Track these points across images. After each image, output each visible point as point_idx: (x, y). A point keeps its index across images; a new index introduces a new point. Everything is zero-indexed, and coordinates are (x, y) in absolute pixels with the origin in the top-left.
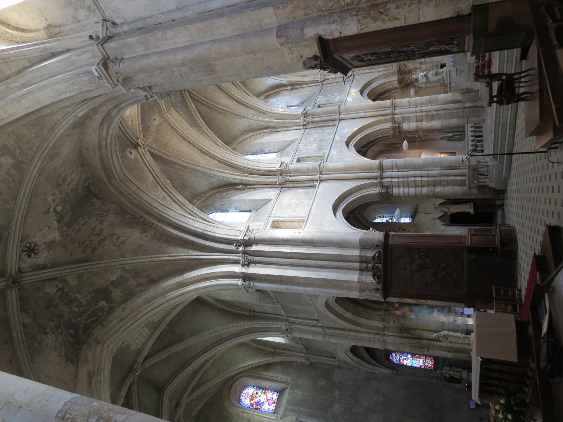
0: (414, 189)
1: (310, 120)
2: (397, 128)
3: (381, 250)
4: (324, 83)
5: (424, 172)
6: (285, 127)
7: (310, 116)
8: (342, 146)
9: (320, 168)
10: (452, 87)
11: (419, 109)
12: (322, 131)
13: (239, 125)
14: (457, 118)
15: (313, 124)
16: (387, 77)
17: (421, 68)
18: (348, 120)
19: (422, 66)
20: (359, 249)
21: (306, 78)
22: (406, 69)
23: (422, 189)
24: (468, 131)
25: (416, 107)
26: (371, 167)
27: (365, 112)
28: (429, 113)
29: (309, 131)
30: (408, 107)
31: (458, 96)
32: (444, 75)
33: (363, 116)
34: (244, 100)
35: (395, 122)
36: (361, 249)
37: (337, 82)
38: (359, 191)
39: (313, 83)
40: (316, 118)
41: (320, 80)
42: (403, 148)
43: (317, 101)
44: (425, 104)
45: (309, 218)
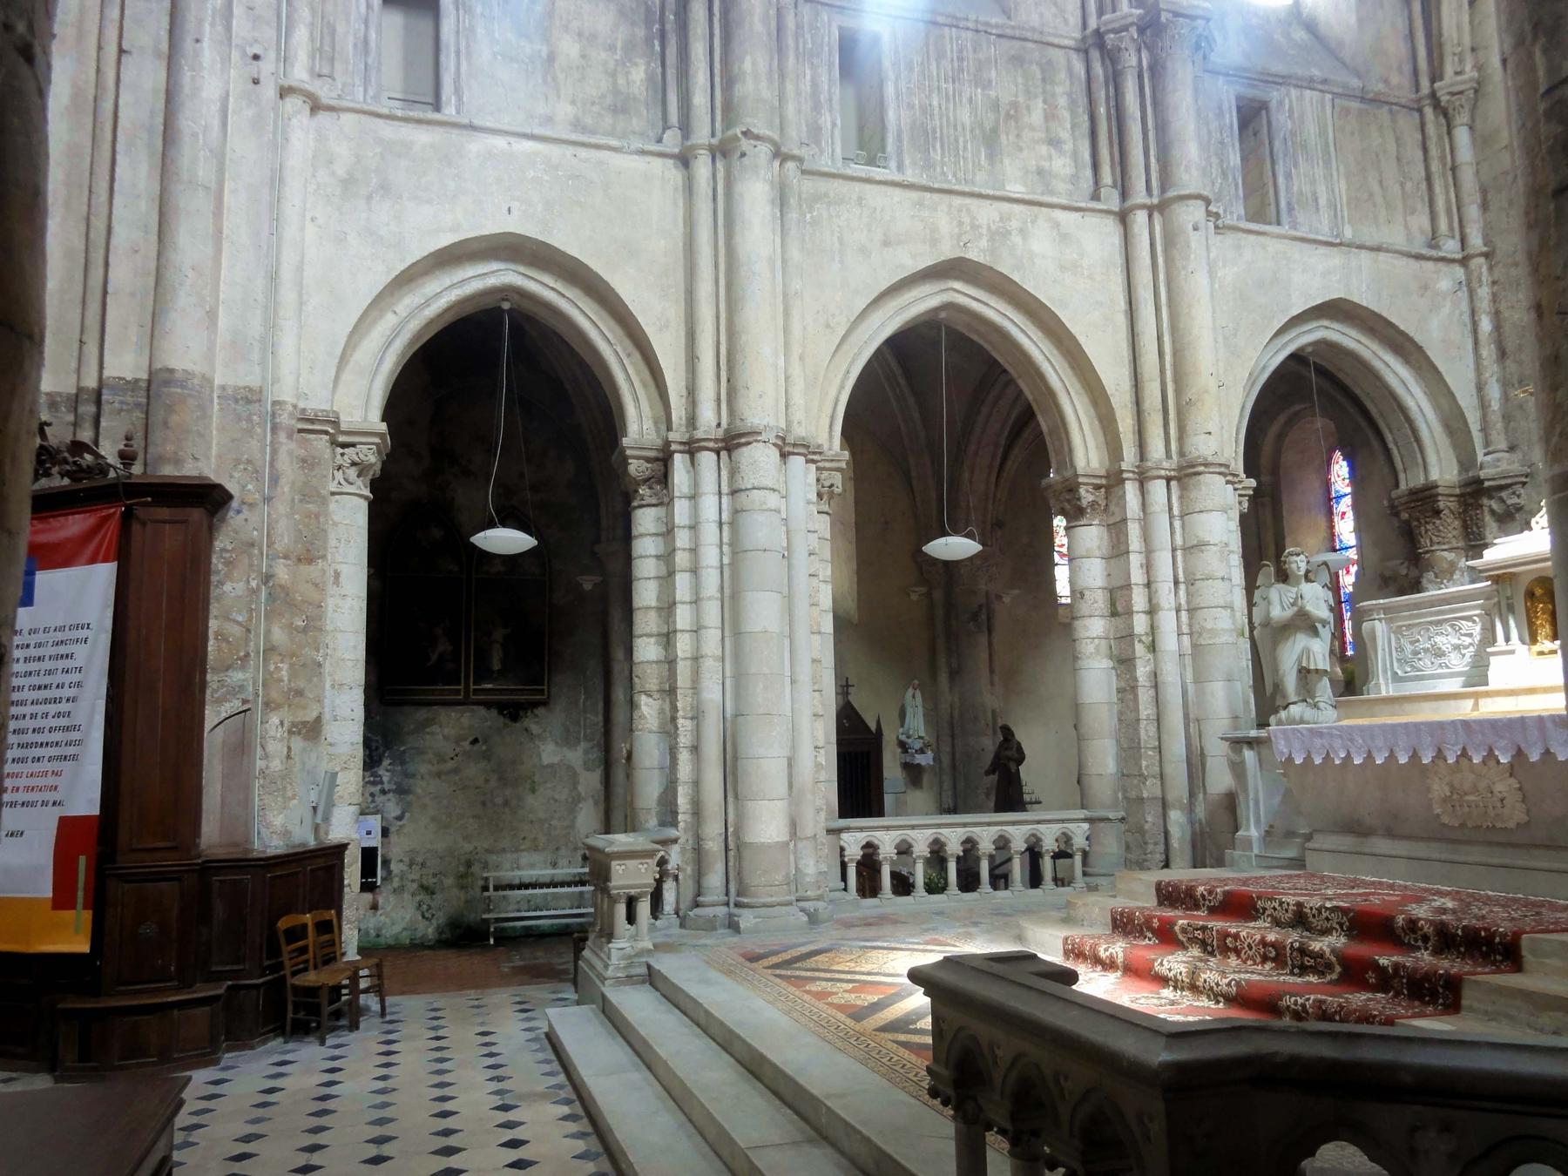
0: (654, 604)
1: (1129, 59)
3: (112, 474)
4: (1429, 112)
5: (712, 641)
8: (934, 242)
10: (1240, 752)
12: (1065, 135)
16: (1450, 430)
18: (1119, 260)
20: (145, 376)
22: (1488, 518)
23: (649, 635)
24: (1039, 822)
25: (1176, 583)
30: (1179, 541)
31: (1220, 780)
36: (144, 385)
37: (1428, 178)
38: (637, 356)
42: (944, 534)
43: (1294, 92)
44: (1190, 626)
45: (425, 127)
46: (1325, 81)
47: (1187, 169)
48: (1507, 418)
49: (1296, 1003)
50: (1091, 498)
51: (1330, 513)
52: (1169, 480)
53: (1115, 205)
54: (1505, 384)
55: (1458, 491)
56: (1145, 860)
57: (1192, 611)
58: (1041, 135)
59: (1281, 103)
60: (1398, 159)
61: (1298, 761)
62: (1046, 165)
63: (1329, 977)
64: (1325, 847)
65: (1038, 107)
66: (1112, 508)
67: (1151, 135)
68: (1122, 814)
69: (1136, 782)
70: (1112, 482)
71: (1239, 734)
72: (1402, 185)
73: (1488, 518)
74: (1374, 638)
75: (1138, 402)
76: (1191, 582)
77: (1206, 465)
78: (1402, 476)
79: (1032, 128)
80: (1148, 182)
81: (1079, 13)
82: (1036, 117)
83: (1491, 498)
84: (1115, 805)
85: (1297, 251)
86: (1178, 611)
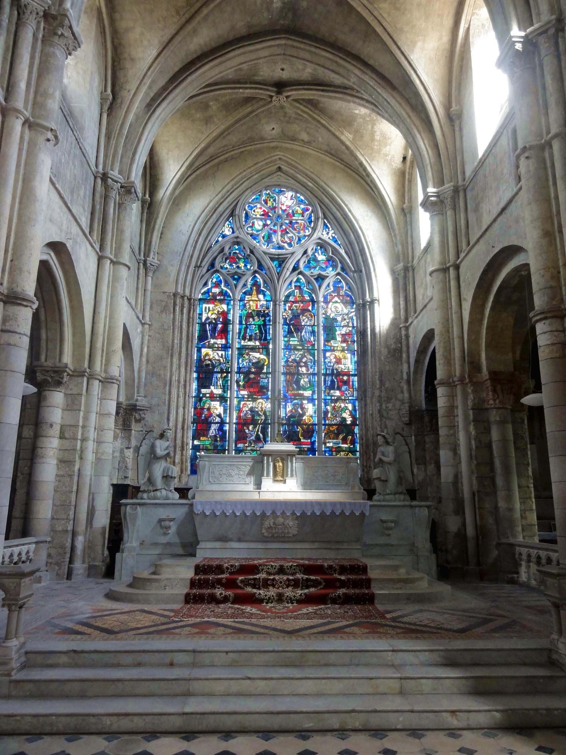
1: (114, 194)
2: (57, 378)
4: (141, 265)
6: (108, 137)
7: (121, 199)
9: (47, 129)
11: (92, 434)
13: (142, 34)
14: (53, 518)
15: (101, 197)
17: (128, 448)
19: (131, 450)
21: (157, 237)
25: (95, 428)
26: (21, 270)
27: (106, 317)
28: (77, 456)
32: (164, 492)
33: (97, 311)
34: (190, 79)
39: (145, 245)
40: (114, 209)
41: (150, 259)
44: (97, 450)
48: (145, 385)
49: (335, 595)
54: (147, 373)
55: (125, 407)
56: (64, 562)
63: (319, 587)
64: (207, 547)
66: (70, 387)
69: (63, 522)
73: (133, 420)
77: (117, 380)
83: (136, 413)
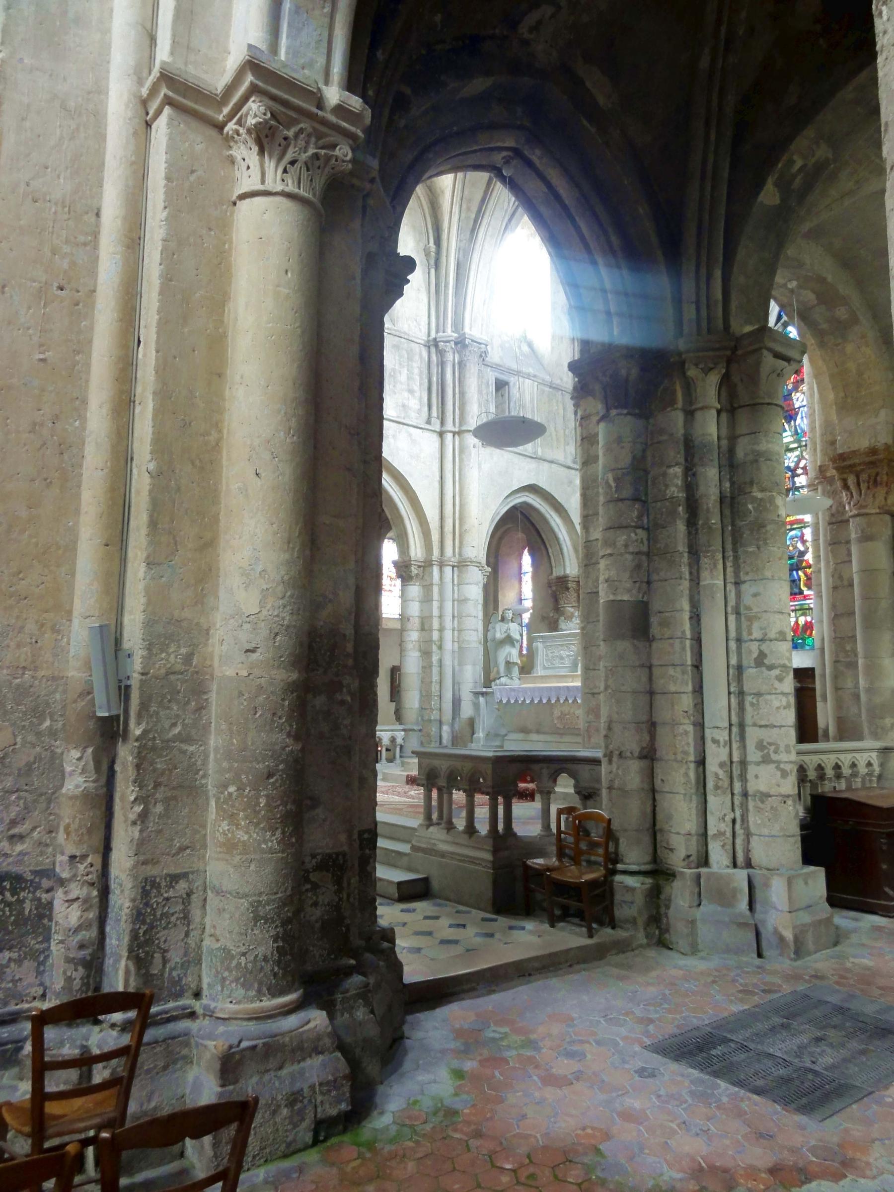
1: (449, 357)
12: (416, 388)
18: (438, 455)
25: (453, 617)
29: (421, 355)
30: (456, 596)
31: (467, 711)
33: (444, 492)
35: (424, 567)
43: (521, 379)
44: (458, 638)
46: (535, 376)
47: (472, 416)
50: (416, 572)
51: (520, 581)
52: (453, 567)
53: (437, 428)
57: (460, 631)
58: (405, 387)
59: (515, 384)
60: (564, 418)
61: (504, 702)
62: (406, 402)
65: (405, 371)
66: (426, 577)
67: (457, 396)
68: (420, 728)
70: (427, 564)
71: (479, 690)
72: (565, 430)
74: (537, 649)
75: (442, 527)
76: (460, 617)
78: (554, 569)
79: (401, 383)
80: (454, 419)
81: (427, 327)
82: (403, 377)
84: (417, 724)
85: (516, 459)
86: (453, 630)
